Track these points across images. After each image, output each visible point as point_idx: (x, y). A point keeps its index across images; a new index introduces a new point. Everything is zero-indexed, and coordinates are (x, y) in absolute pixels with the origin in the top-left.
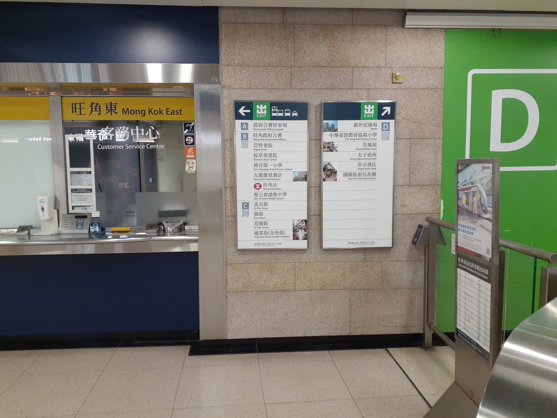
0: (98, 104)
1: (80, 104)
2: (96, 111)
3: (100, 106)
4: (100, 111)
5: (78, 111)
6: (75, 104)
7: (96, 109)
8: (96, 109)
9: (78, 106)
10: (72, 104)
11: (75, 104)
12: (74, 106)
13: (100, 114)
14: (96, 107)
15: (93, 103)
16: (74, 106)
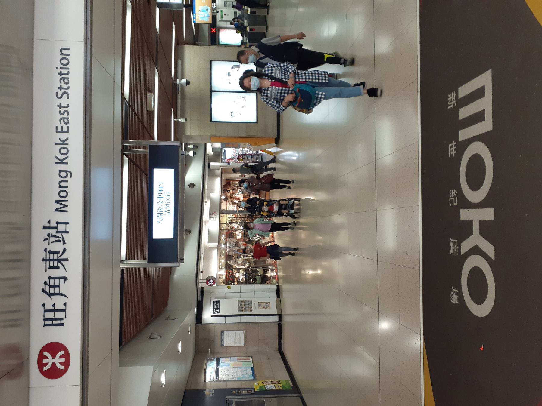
0: (45, 283)
1: (45, 311)
2: (58, 286)
3: (50, 278)
4: (59, 278)
5: (58, 315)
6: (45, 319)
7: (54, 286)
8: (54, 286)
9: (49, 315)
10: (45, 325)
11: (45, 319)
12: (50, 322)
13: (65, 279)
14: (50, 286)
15: (44, 291)
16: (50, 322)
